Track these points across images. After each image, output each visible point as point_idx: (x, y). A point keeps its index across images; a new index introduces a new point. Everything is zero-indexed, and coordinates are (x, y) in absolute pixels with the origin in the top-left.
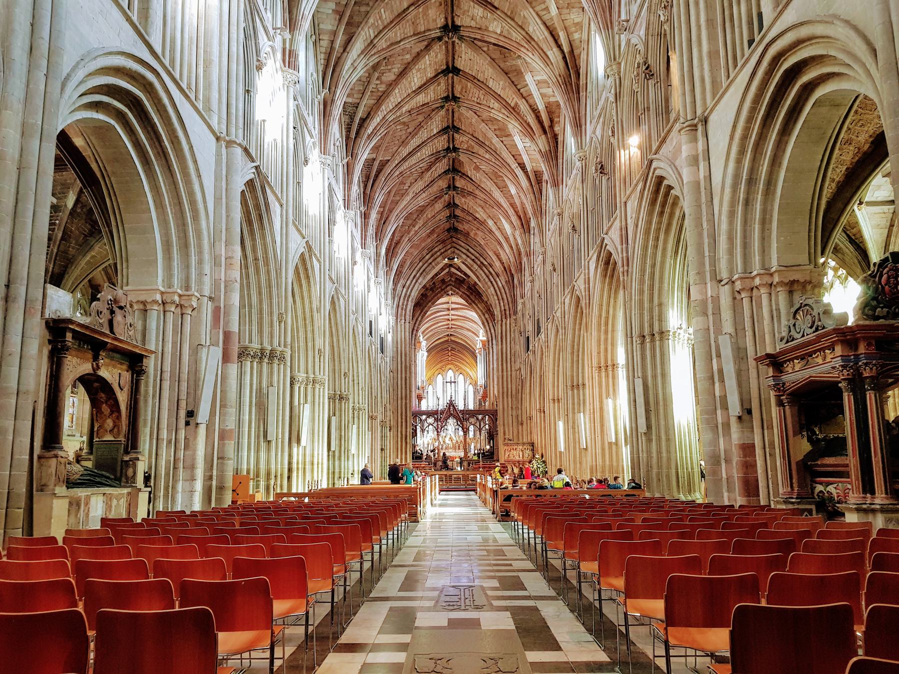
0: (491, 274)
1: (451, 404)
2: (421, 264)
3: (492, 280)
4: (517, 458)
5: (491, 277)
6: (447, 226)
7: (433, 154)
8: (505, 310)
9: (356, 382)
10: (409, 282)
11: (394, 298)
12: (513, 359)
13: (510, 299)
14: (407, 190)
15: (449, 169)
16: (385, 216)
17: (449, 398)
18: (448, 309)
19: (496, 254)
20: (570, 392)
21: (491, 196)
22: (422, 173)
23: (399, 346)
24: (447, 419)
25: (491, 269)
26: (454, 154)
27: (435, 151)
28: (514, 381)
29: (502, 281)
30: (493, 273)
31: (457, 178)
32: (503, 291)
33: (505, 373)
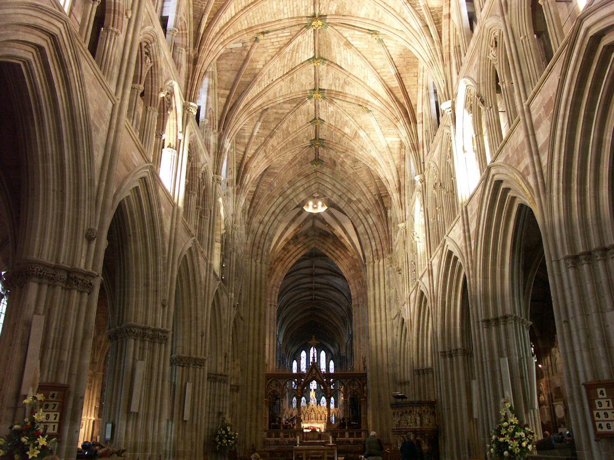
0: (359, 210)
1: (314, 367)
2: (281, 199)
3: (362, 217)
4: (413, 426)
5: (360, 214)
6: (312, 157)
7: (293, 18)
8: (377, 250)
9: (151, 288)
10: (267, 218)
11: (247, 233)
12: (388, 306)
13: (383, 236)
14: (260, 70)
15: (314, 57)
16: (232, 100)
17: (311, 360)
18: (312, 275)
19: (365, 185)
20: (571, 272)
21: (365, 84)
22: (281, 48)
23: (252, 290)
24: (307, 384)
25: (360, 206)
26: (320, 23)
27: (296, 15)
28: (389, 331)
29: (372, 219)
30: (363, 209)
31: (322, 68)
32: (374, 228)
33: (378, 323)
